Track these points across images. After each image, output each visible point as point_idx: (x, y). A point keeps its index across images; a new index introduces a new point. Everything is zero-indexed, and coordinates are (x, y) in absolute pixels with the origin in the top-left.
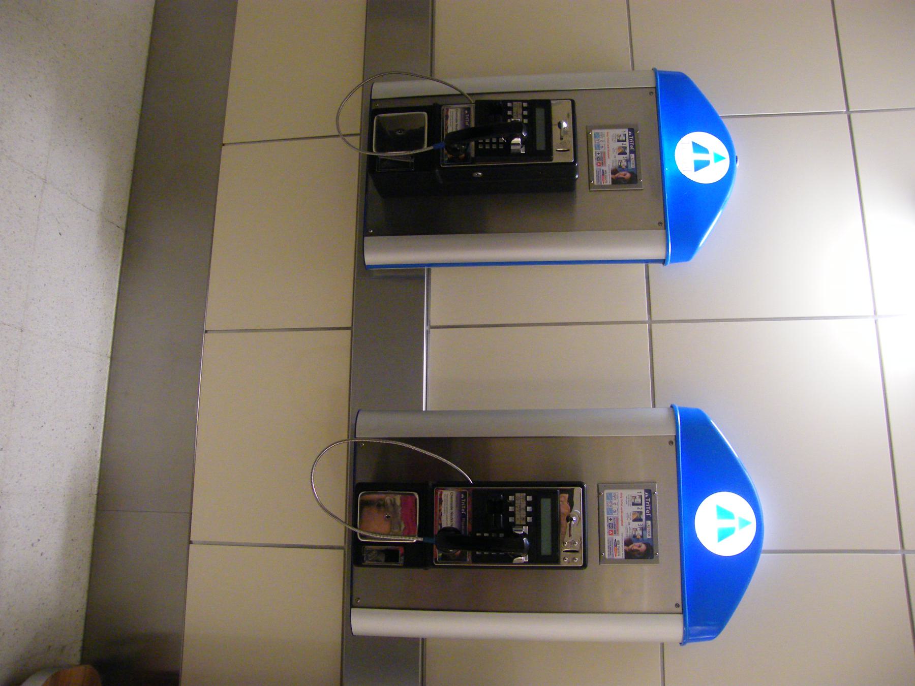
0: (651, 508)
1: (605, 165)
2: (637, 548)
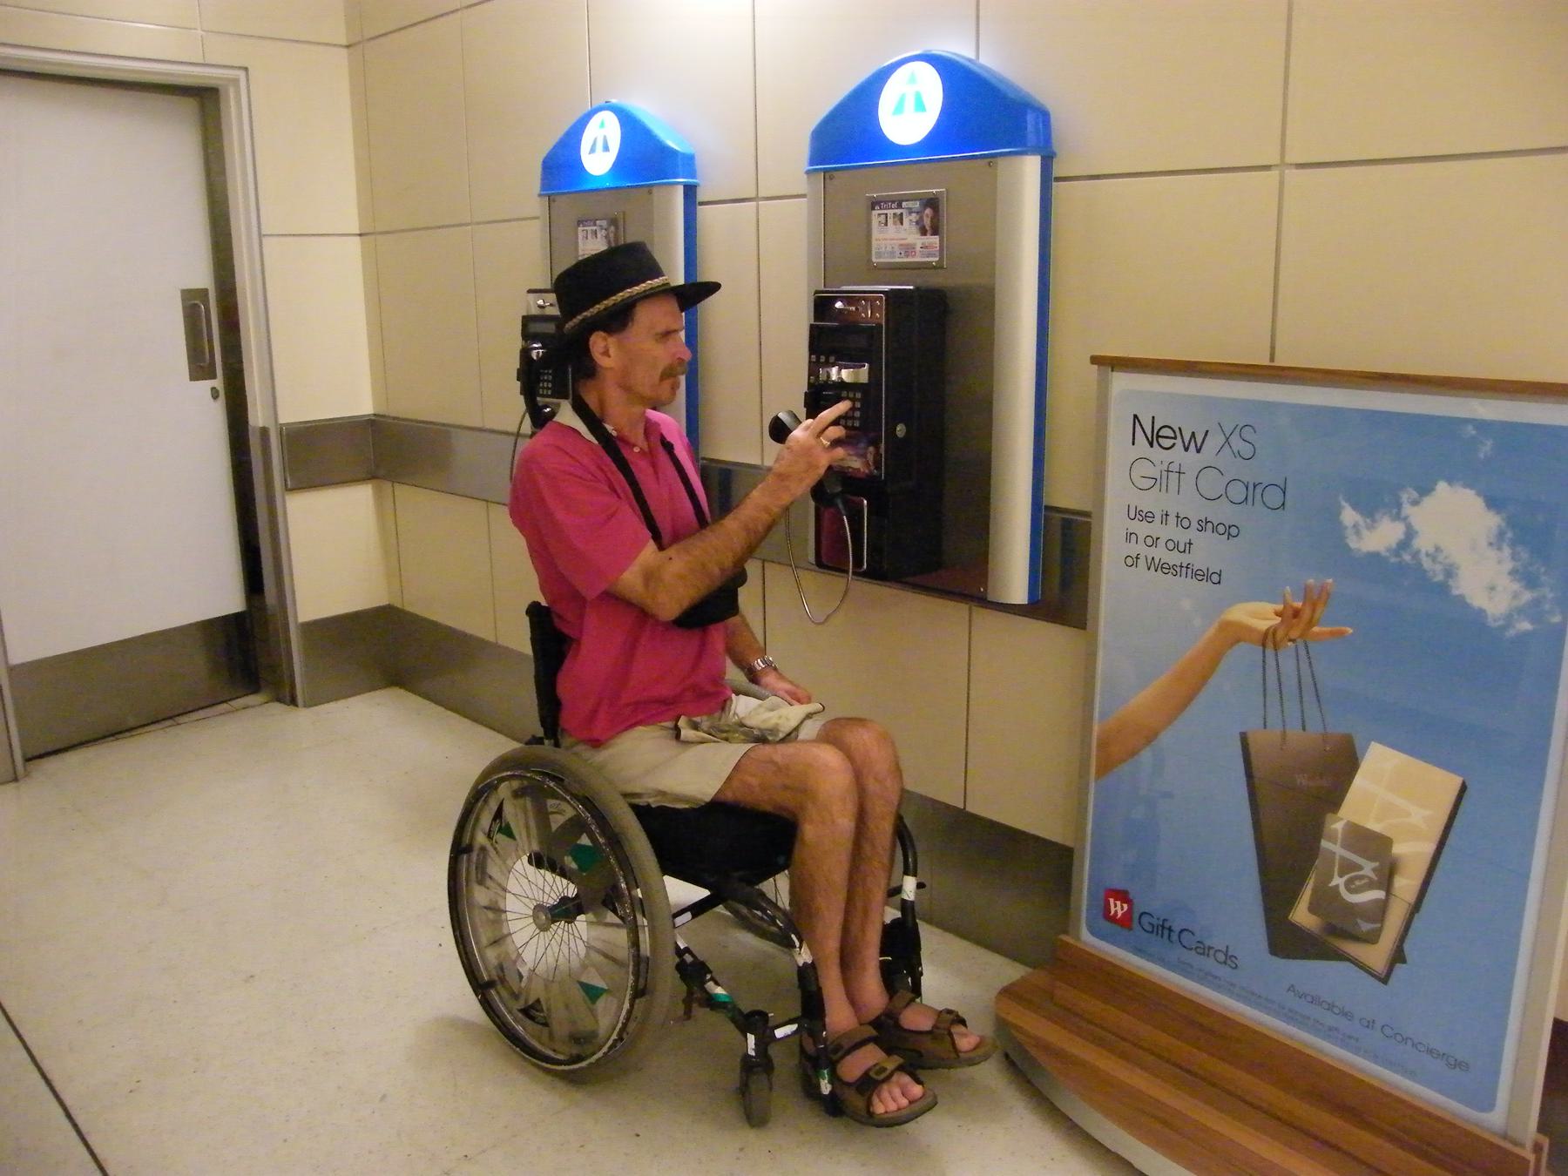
0: (889, 202)
2: (929, 219)
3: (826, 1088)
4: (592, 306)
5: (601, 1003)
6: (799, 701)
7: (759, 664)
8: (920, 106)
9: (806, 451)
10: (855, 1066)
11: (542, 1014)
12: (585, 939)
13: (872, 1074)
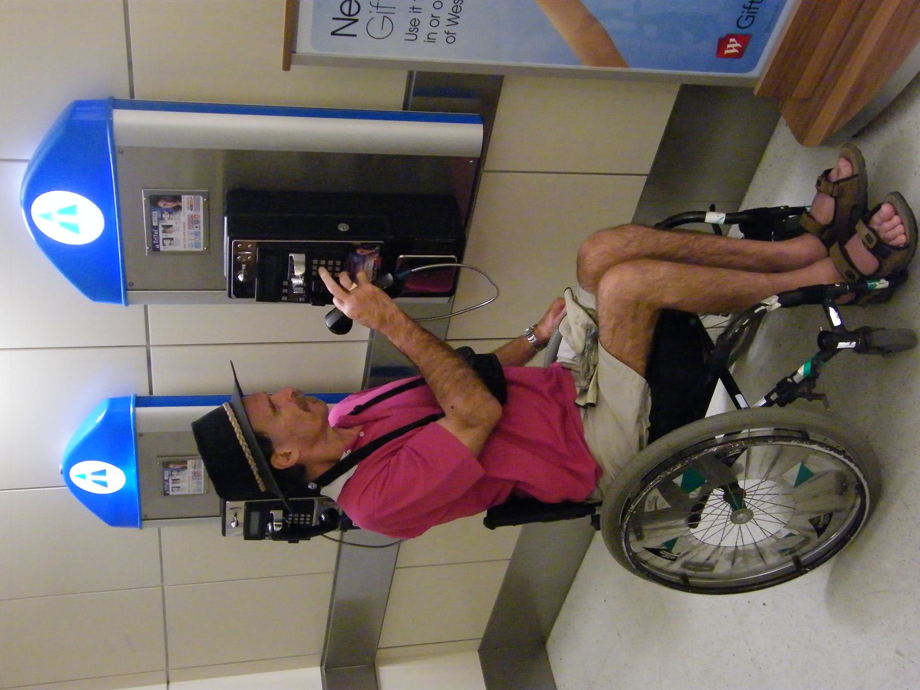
0: (152, 236)
1: (188, 215)
2: (168, 203)
3: (883, 284)
4: (249, 466)
5: (813, 469)
6: (562, 307)
7: (532, 339)
8: (71, 210)
9: (361, 303)
10: (865, 260)
11: (822, 518)
12: (759, 481)
13: (871, 246)
